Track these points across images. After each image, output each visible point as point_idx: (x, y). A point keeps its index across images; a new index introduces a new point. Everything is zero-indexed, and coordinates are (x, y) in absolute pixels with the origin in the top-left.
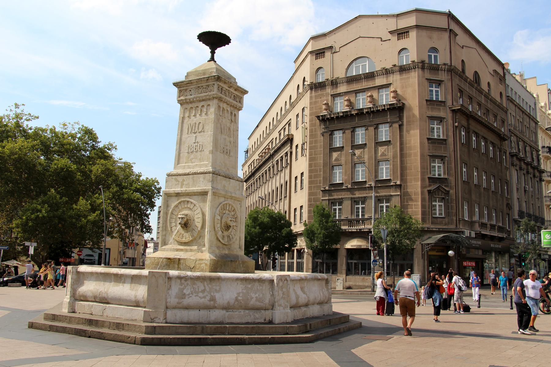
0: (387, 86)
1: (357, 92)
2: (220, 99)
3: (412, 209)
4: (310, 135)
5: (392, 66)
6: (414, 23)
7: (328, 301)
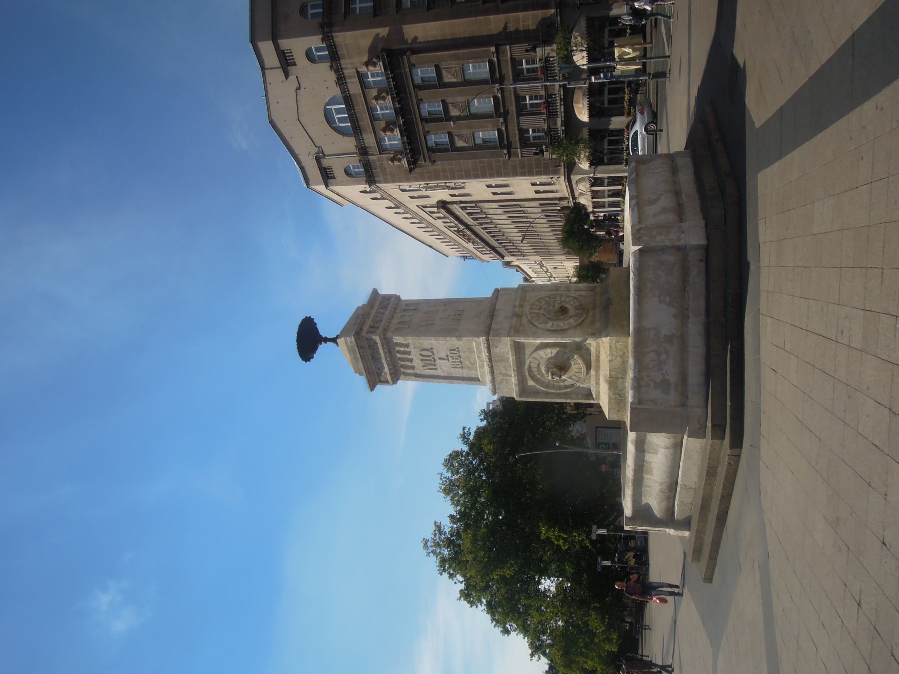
0: (361, 77)
1: (373, 118)
2: (385, 330)
3: (529, 24)
4: (436, 180)
5: (333, 71)
6: (270, 44)
7: (671, 158)
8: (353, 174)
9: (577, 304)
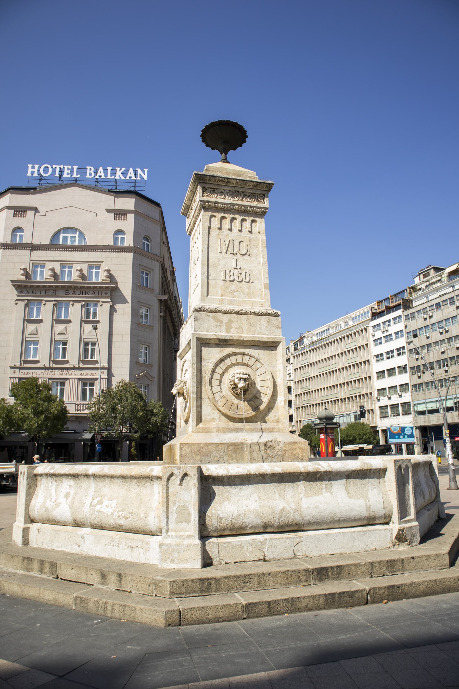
6: (133, 208)
8: (15, 233)
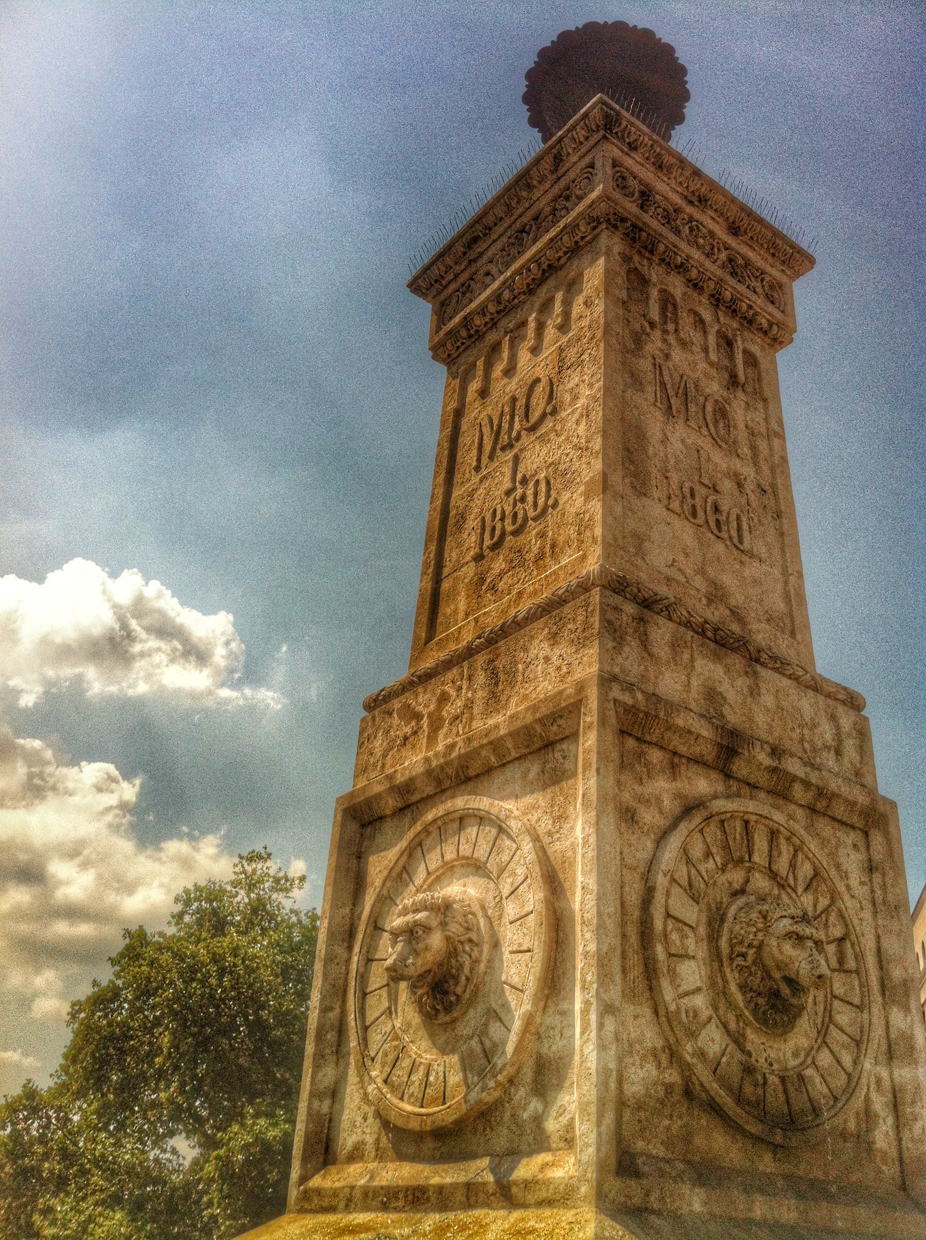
9: (818, 1088)
